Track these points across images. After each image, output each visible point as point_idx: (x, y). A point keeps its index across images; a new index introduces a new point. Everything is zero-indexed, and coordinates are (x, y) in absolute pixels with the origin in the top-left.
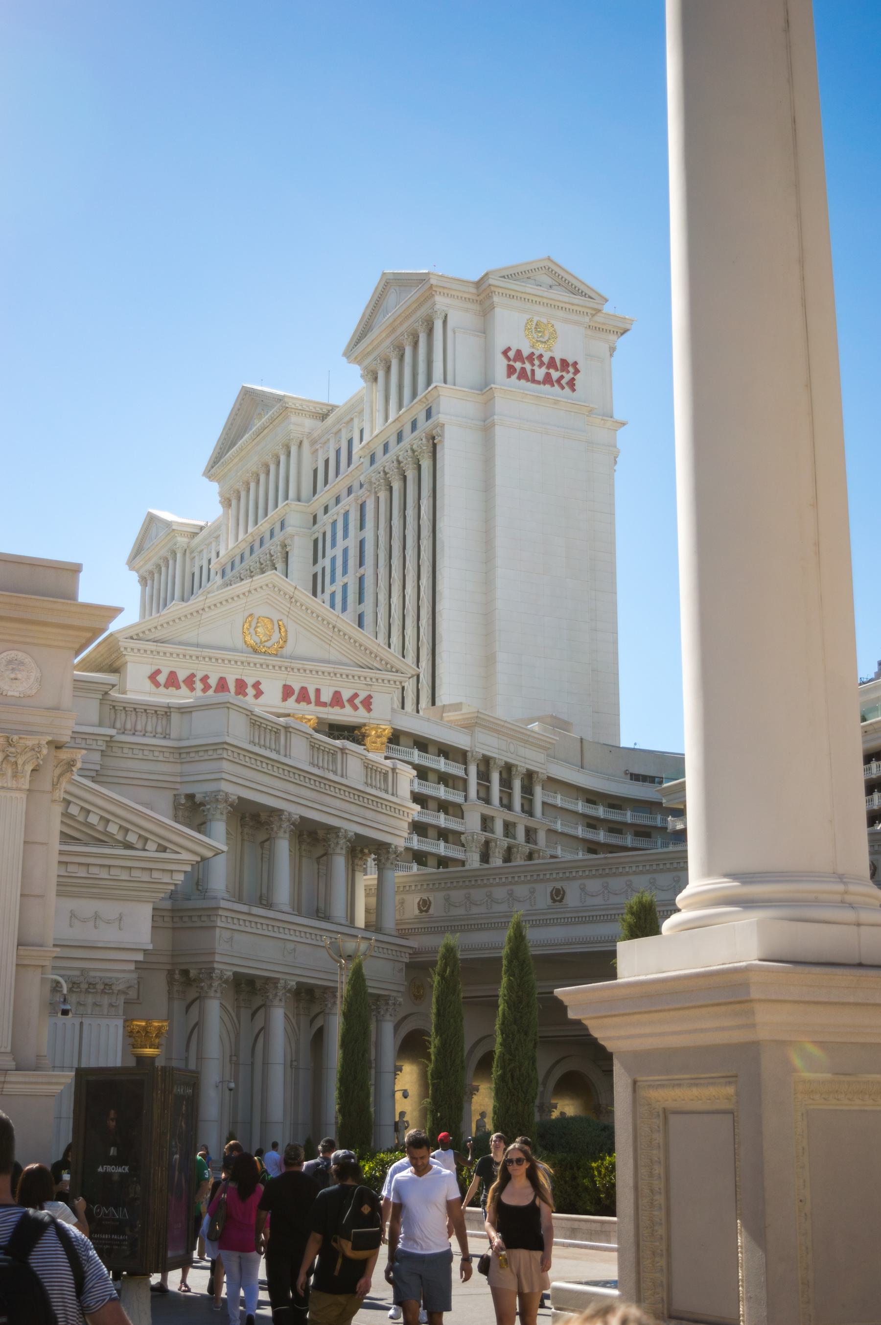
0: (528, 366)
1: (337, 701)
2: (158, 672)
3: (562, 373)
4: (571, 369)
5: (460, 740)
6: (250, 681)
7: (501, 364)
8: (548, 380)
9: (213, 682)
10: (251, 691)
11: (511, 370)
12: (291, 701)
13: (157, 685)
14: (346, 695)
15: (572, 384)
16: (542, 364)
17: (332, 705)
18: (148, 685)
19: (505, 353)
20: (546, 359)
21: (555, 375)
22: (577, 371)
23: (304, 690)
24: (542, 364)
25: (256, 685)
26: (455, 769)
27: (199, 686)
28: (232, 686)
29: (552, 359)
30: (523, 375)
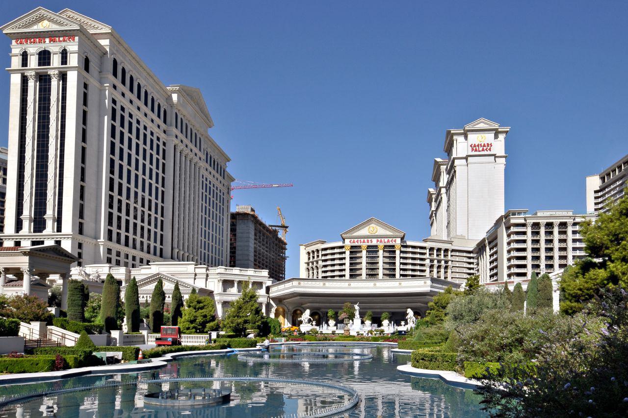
2: (351, 241)
10: (370, 242)
12: (379, 243)
18: (349, 243)
27: (359, 242)
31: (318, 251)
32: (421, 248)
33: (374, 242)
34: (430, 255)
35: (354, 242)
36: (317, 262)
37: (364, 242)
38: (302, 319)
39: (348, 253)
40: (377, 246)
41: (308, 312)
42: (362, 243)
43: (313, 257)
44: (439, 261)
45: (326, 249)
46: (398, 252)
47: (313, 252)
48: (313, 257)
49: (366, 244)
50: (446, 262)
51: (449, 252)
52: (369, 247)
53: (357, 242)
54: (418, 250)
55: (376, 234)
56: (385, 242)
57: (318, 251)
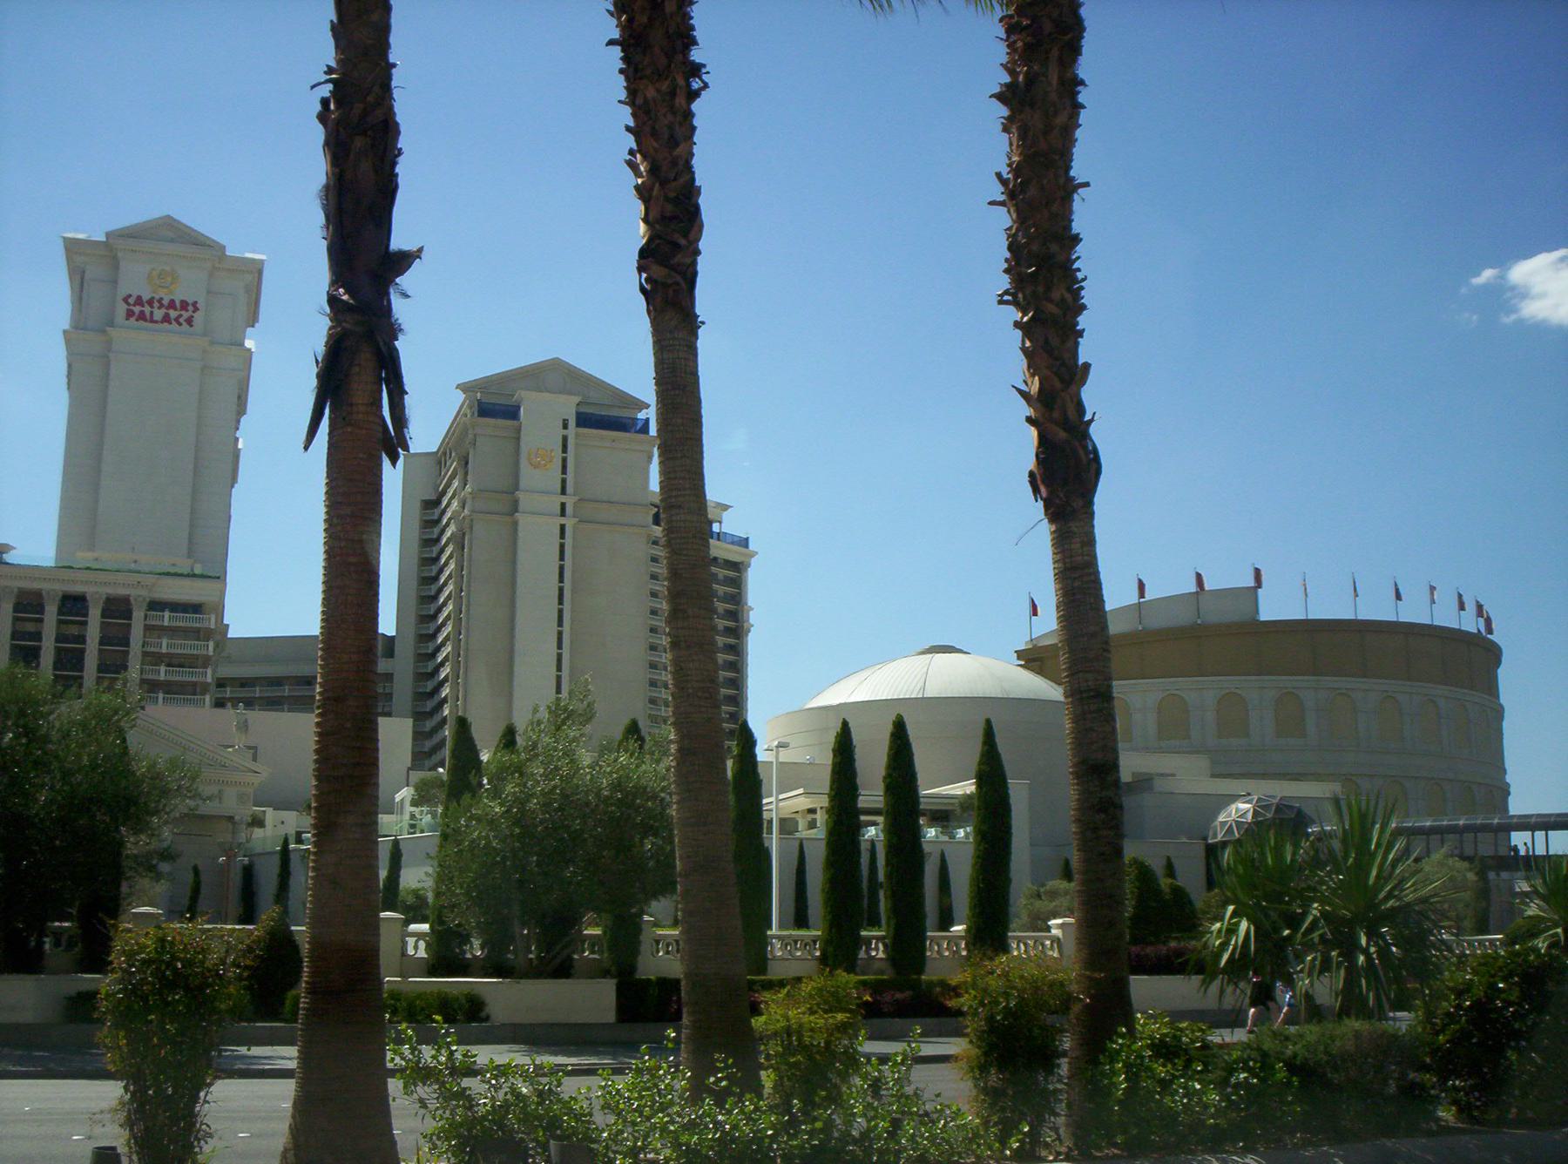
0: (147, 309)
3: (180, 312)
4: (190, 308)
7: (122, 309)
8: (166, 319)
11: (130, 314)
15: (189, 321)
16: (161, 306)
19: (126, 300)
20: (166, 302)
21: (173, 314)
22: (196, 309)
30: (142, 317)
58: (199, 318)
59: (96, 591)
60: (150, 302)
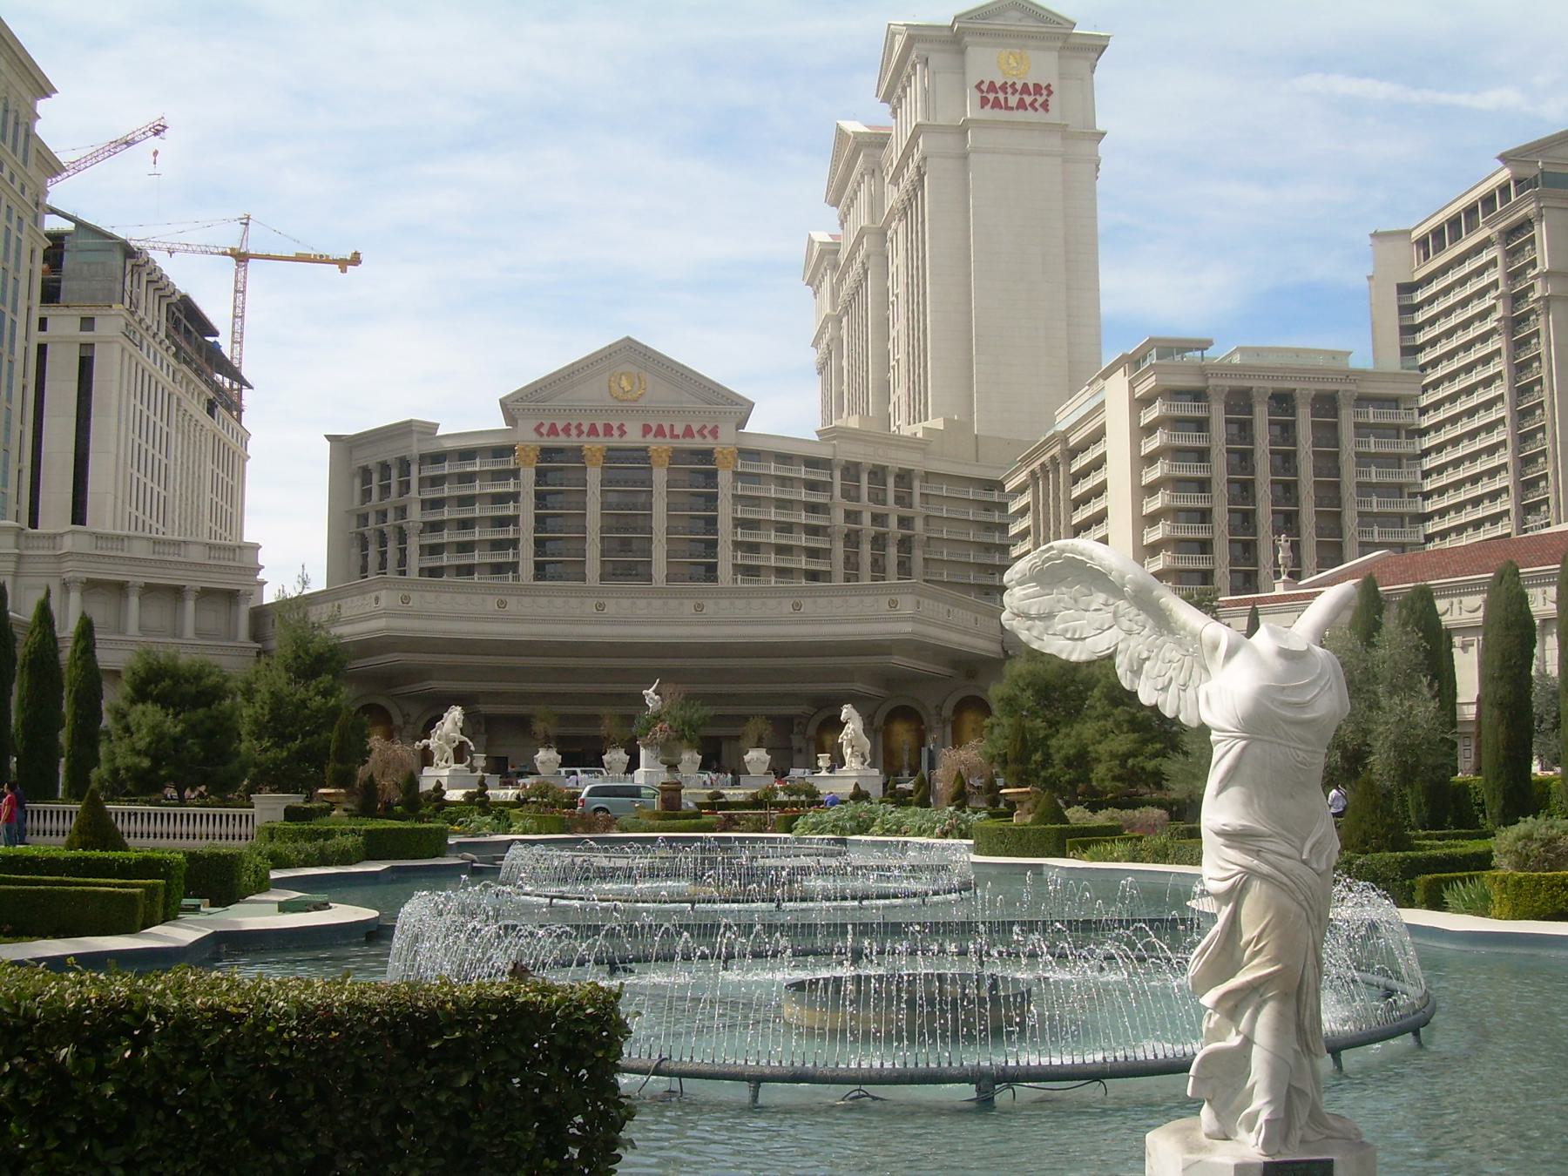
0: (1001, 96)
1: (688, 432)
3: (1036, 95)
4: (1044, 92)
5: (824, 452)
6: (615, 425)
7: (972, 98)
8: (1021, 105)
9: (585, 428)
10: (616, 432)
13: (541, 435)
14: (695, 428)
15: (1045, 105)
16: (1015, 92)
17: (684, 436)
18: (534, 436)
19: (978, 87)
20: (1019, 87)
21: (1028, 100)
23: (660, 427)
24: (1015, 92)
25: (621, 427)
26: (820, 476)
27: (574, 432)
28: (601, 430)
29: (1025, 85)
30: (996, 104)
31: (404, 465)
32: (812, 463)
33: (634, 437)
34: (846, 494)
35: (553, 430)
36: (402, 511)
37: (593, 431)
38: (433, 743)
39: (528, 475)
40: (645, 449)
41: (455, 714)
42: (584, 438)
43: (385, 490)
44: (878, 519)
45: (438, 458)
46: (725, 478)
47: (385, 468)
48: (385, 490)
49: (602, 442)
50: (904, 522)
51: (916, 484)
52: (612, 455)
53: (567, 430)
54: (803, 473)
55: (641, 403)
56: (673, 436)
57: (404, 465)
58: (1053, 101)
59: (1305, 389)
60: (1004, 88)
